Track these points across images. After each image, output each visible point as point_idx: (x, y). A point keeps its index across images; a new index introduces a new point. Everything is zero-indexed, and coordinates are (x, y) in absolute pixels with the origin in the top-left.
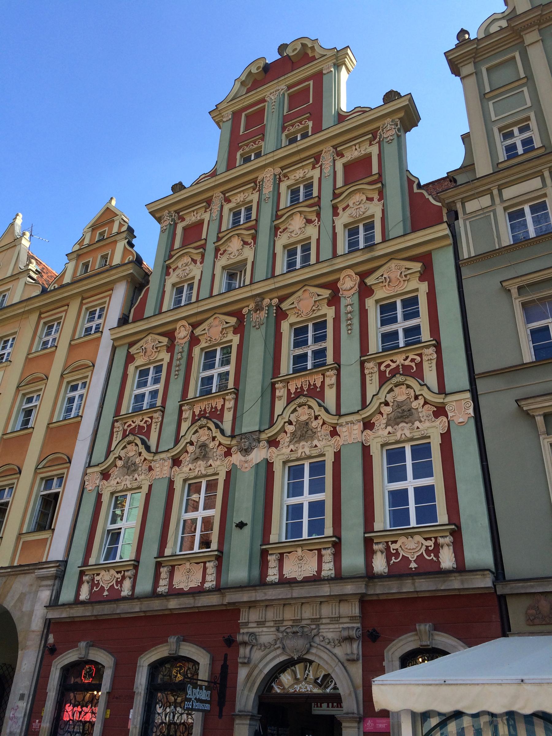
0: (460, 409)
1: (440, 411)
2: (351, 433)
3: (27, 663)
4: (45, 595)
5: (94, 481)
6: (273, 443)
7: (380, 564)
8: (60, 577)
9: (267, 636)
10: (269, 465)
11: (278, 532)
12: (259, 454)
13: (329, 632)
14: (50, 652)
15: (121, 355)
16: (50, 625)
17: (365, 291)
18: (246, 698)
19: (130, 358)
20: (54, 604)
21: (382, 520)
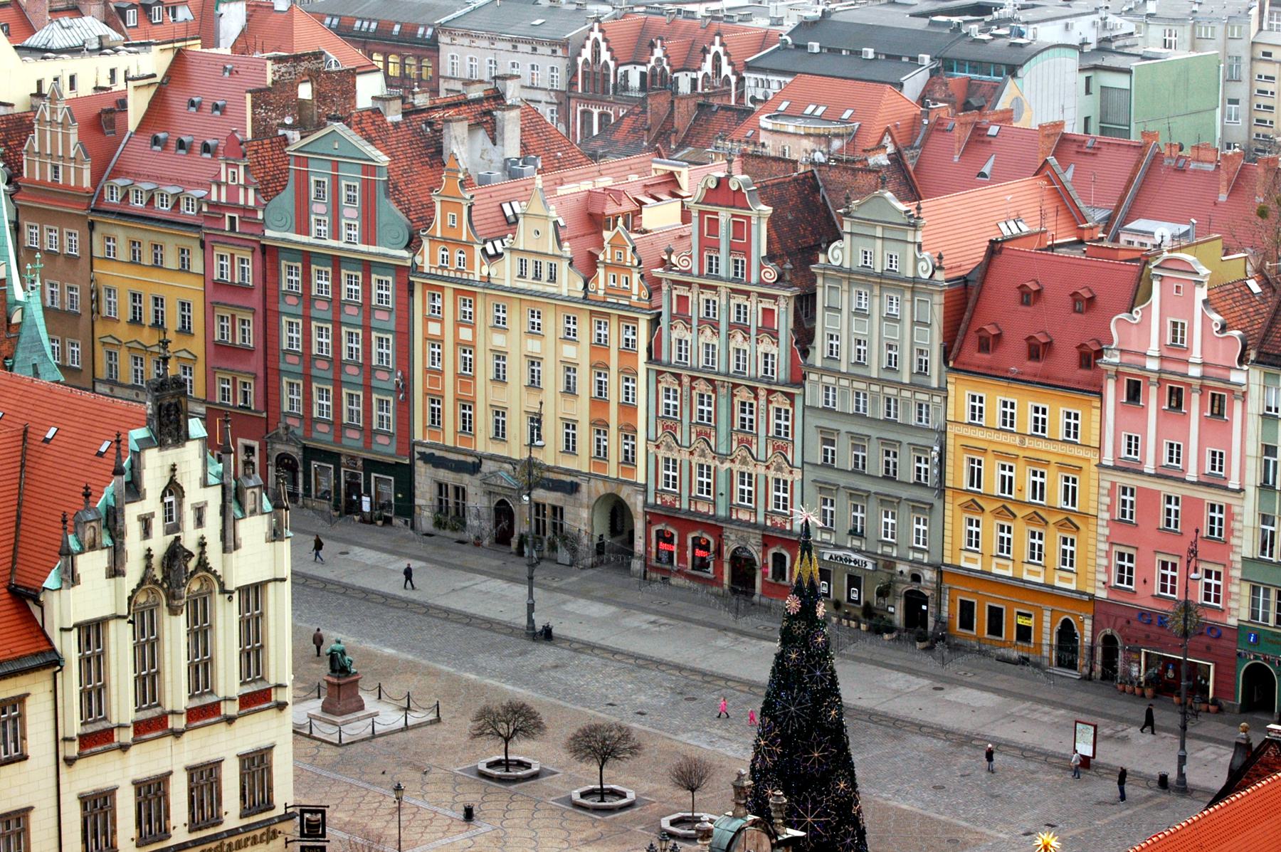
0: (797, 475)
1: (791, 472)
2: (761, 470)
3: (639, 526)
4: (641, 498)
5: (652, 449)
6: (733, 461)
7: (769, 523)
8: (646, 491)
9: (733, 537)
10: (732, 471)
11: (736, 500)
12: (727, 465)
13: (753, 541)
14: (648, 524)
15: (653, 376)
16: (646, 513)
17: (769, 402)
18: (727, 556)
19: (658, 382)
20: (645, 502)
21: (771, 507)
